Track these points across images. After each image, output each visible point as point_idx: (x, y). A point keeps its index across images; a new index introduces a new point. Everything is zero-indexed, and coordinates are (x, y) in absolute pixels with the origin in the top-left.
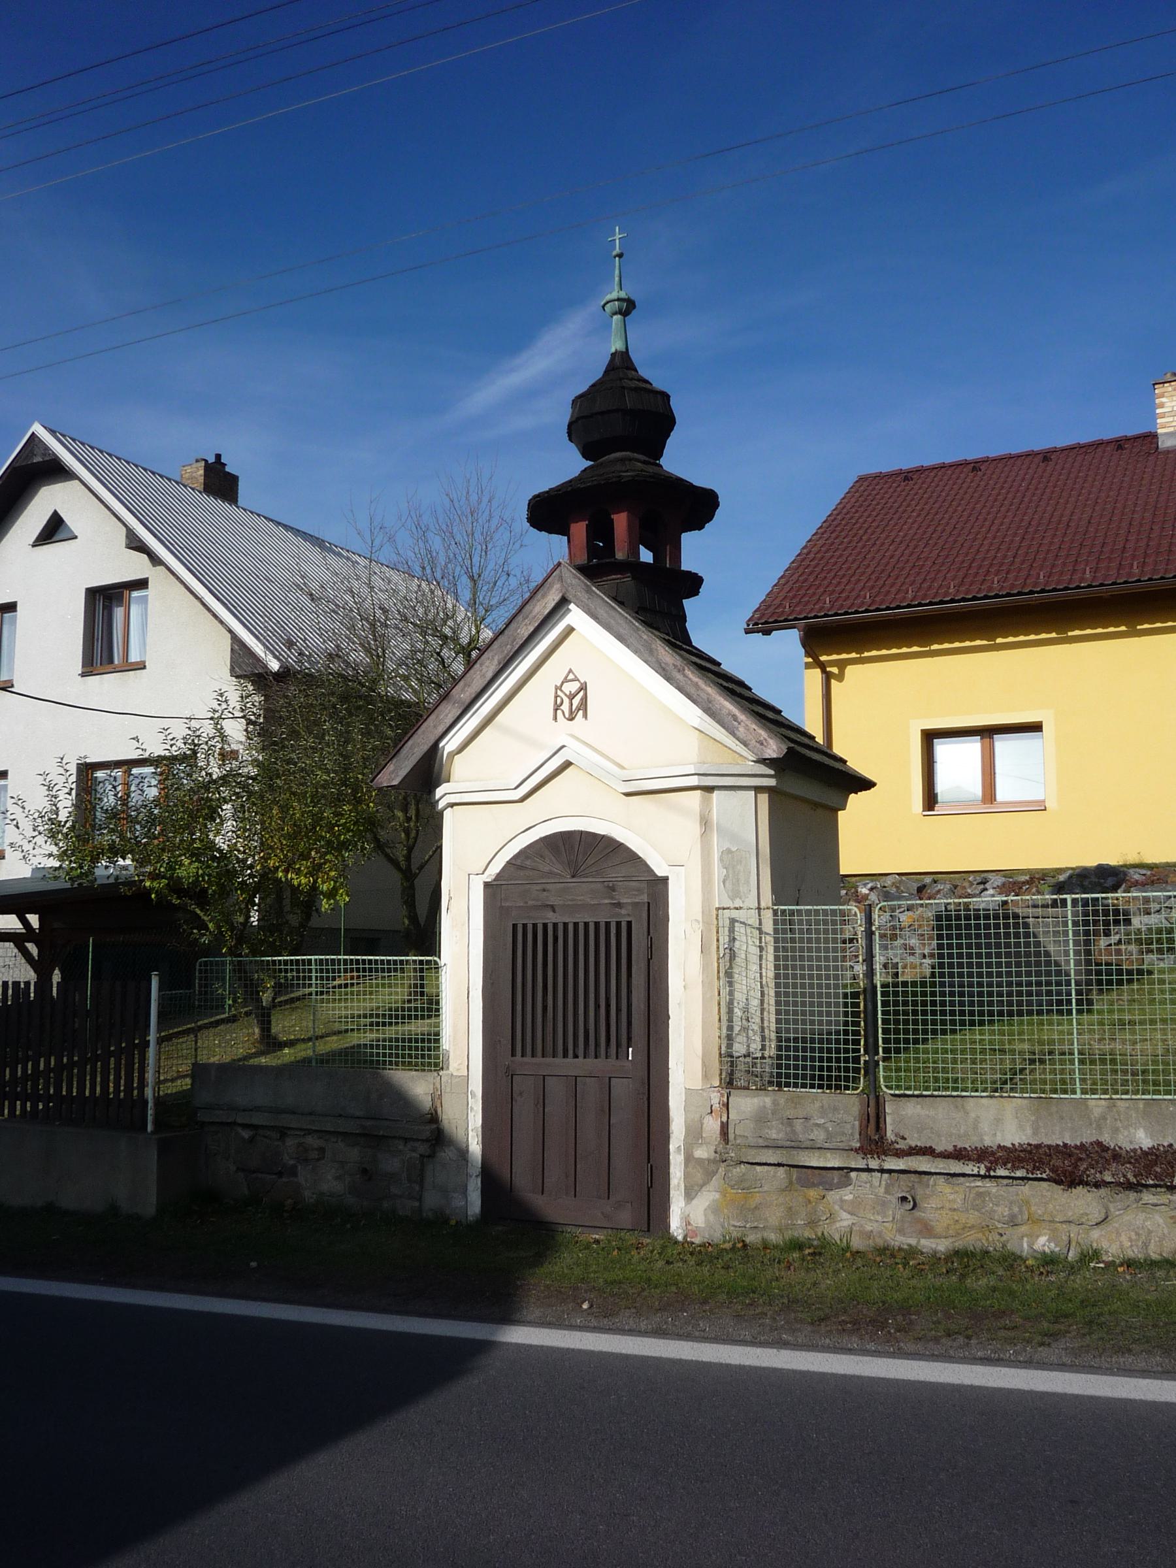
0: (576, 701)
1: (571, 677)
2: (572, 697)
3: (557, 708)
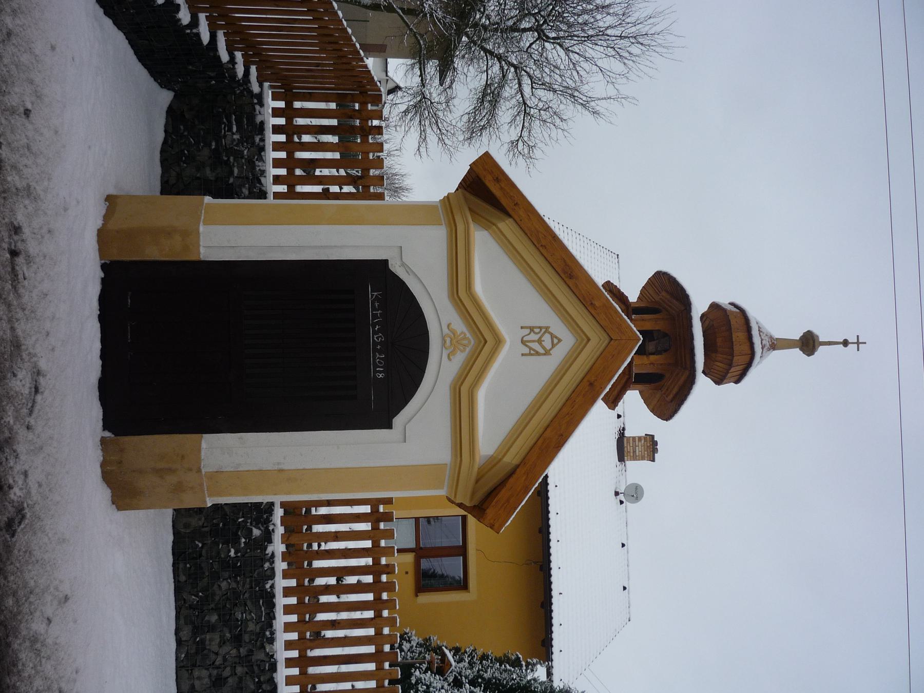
0: (536, 346)
1: (556, 341)
2: (540, 341)
3: (532, 329)
